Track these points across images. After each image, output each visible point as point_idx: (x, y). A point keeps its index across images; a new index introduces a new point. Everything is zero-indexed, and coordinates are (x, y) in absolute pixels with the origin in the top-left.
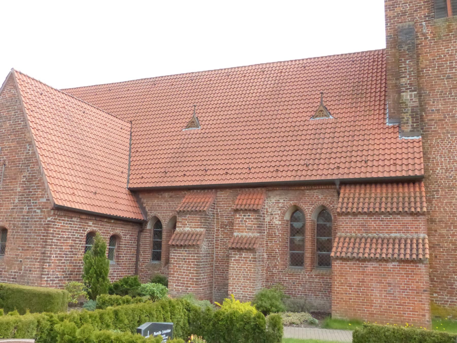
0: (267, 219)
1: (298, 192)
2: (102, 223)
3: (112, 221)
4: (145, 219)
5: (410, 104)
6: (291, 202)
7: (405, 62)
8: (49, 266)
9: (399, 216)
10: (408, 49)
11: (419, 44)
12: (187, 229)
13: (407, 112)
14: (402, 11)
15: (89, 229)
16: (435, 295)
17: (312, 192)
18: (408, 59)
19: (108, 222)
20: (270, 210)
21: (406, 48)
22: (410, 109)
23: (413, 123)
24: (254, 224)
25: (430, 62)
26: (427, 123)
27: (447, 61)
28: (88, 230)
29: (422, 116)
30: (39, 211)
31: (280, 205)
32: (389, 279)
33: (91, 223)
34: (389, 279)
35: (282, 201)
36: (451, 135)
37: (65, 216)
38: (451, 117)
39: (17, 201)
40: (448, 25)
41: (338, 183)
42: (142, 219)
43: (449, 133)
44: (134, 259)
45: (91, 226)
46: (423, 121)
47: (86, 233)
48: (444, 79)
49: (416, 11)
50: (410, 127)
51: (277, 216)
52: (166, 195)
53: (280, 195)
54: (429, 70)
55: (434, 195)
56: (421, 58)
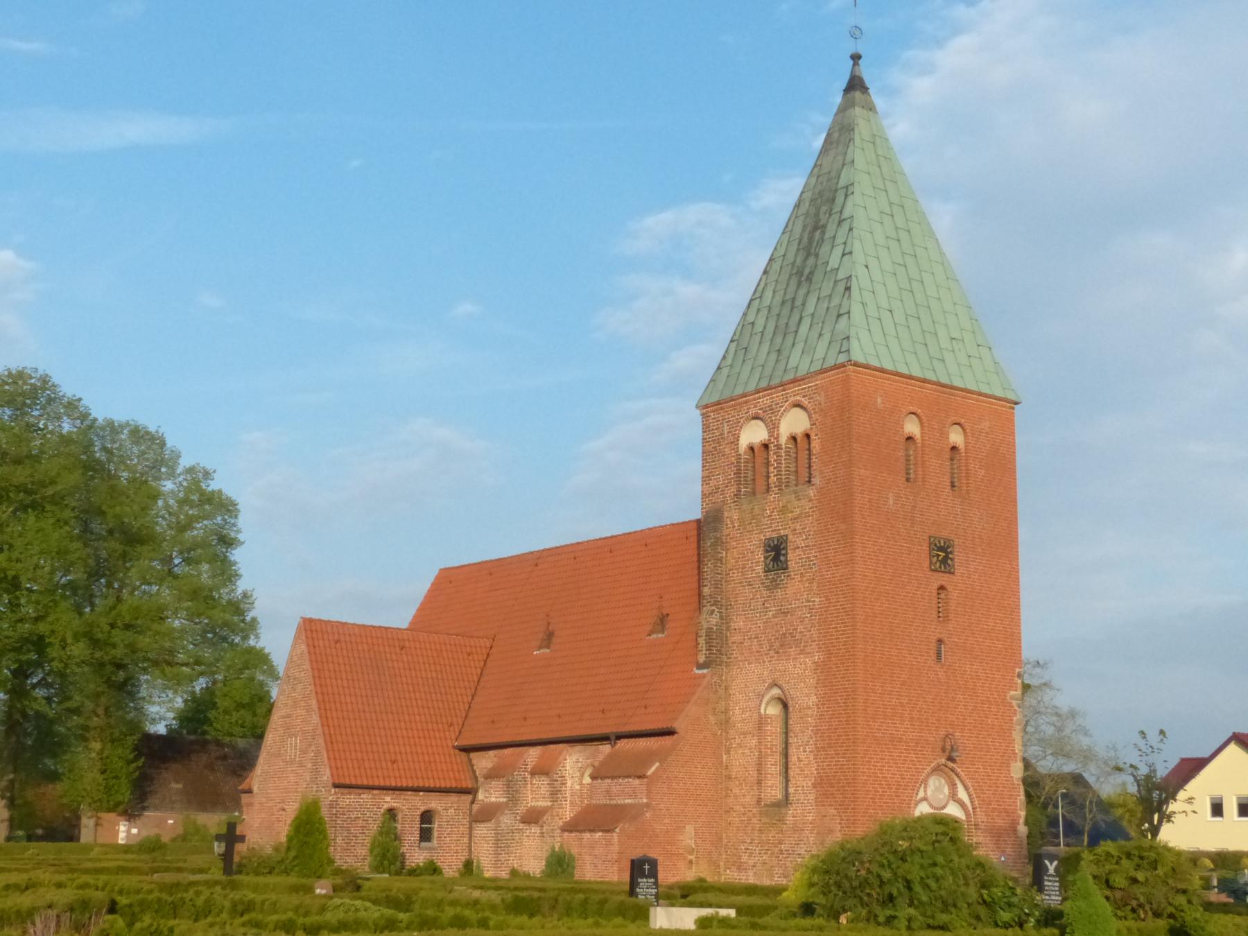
0: (569, 783)
1: (594, 748)
2: (407, 797)
3: (421, 793)
4: (475, 786)
5: (705, 626)
6: (589, 761)
7: (707, 564)
8: (335, 849)
9: (631, 780)
10: (710, 546)
11: (727, 535)
12: (493, 799)
13: (701, 636)
14: (715, 486)
15: (386, 806)
16: (728, 871)
17: (604, 746)
18: (710, 561)
19: (416, 796)
20: (571, 772)
21: (709, 544)
22: (704, 631)
23: (707, 650)
24: (547, 791)
25: (736, 562)
26: (730, 647)
27: (748, 560)
28: (384, 807)
29: (727, 637)
30: (323, 790)
31: (580, 765)
32: (596, 852)
33: (388, 799)
34: (596, 852)
35: (581, 760)
36: (749, 664)
37: (350, 793)
38: (749, 639)
39: (308, 779)
40: (752, 509)
41: (613, 738)
42: (470, 786)
43: (746, 660)
44: (466, 840)
45: (389, 801)
46: (727, 644)
47: (382, 810)
48: (745, 586)
49: (727, 486)
50: (704, 656)
51: (577, 779)
52: (491, 753)
53: (580, 752)
54: (734, 573)
55: (731, 744)
56: (729, 555)
